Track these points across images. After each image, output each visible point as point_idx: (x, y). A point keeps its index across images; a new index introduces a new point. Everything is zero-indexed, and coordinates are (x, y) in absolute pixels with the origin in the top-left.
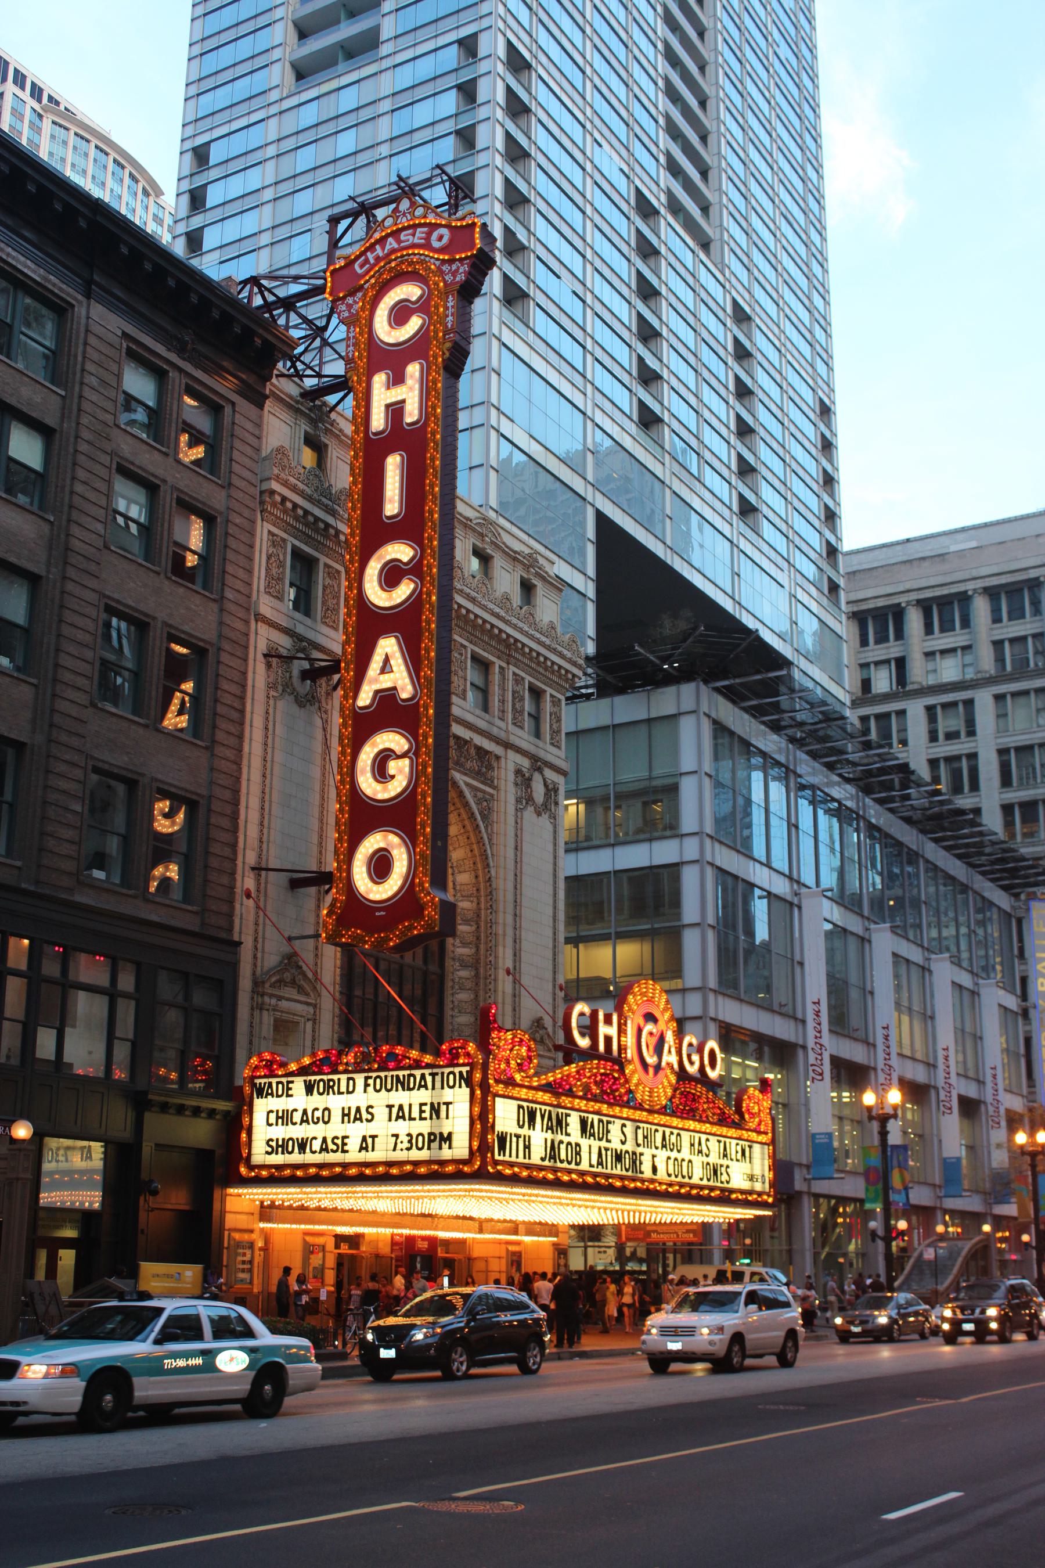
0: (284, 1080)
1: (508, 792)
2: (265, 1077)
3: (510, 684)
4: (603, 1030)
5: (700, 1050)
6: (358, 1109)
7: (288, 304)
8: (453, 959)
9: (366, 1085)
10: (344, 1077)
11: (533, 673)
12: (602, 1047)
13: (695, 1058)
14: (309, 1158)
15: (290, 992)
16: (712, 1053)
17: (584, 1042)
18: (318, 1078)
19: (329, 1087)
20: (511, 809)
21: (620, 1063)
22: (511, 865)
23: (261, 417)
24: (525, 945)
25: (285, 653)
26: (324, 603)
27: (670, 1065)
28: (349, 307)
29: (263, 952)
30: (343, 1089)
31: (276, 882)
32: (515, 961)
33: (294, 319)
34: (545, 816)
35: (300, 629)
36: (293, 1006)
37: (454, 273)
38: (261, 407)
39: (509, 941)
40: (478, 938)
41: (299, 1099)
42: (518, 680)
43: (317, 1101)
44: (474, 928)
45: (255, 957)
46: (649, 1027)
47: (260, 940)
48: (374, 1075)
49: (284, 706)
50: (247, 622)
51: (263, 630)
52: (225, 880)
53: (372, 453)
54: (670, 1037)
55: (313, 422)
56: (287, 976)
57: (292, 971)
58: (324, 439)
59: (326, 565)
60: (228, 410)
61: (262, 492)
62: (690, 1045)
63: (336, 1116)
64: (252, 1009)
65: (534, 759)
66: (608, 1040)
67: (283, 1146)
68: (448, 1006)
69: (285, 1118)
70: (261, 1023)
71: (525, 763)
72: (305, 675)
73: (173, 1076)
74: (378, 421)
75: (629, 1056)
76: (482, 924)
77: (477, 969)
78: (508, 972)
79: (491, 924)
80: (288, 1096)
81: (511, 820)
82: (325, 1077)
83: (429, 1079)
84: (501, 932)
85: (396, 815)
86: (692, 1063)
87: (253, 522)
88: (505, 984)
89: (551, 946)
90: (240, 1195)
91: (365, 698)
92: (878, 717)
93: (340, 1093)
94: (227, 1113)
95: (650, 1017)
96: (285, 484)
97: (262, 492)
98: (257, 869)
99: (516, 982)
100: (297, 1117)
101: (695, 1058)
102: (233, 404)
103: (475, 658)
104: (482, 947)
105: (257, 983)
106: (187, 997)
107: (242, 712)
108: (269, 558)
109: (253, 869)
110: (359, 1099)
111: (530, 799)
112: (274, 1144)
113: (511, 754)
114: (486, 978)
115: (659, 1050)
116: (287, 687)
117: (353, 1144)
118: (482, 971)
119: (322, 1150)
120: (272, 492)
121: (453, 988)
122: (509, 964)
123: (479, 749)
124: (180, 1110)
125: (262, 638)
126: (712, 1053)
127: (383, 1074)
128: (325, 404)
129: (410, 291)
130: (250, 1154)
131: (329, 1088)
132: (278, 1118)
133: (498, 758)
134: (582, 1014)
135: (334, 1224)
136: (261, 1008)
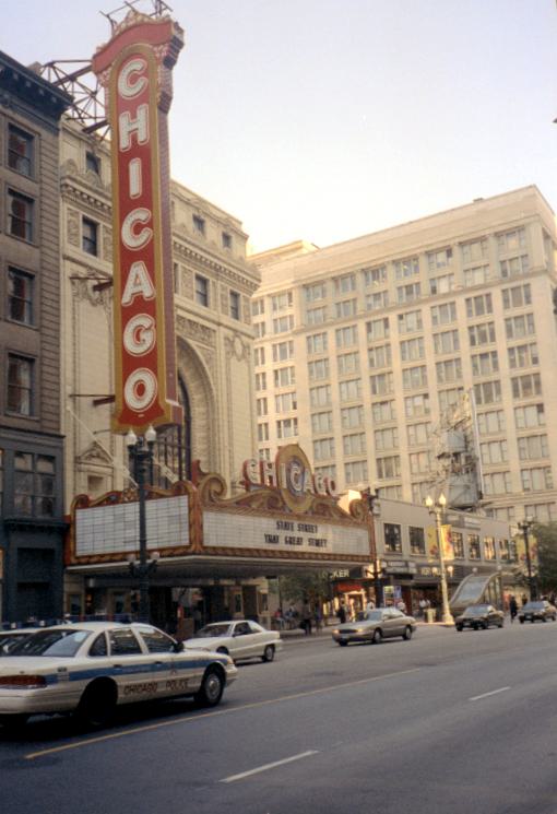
1: (222, 350)
3: (219, 291)
7: (72, 78)
11: (233, 284)
15: (95, 461)
20: (223, 358)
22: (225, 388)
23: (57, 143)
25: (82, 276)
26: (105, 248)
28: (105, 77)
31: (86, 402)
33: (77, 88)
34: (243, 361)
35: (90, 263)
36: (97, 467)
37: (161, 52)
38: (57, 135)
42: (223, 289)
49: (84, 305)
50: (58, 260)
51: (68, 263)
52: (54, 402)
53: (123, 160)
55: (92, 146)
58: (97, 155)
59: (104, 227)
60: (37, 137)
61: (61, 186)
65: (235, 331)
71: (230, 333)
72: (96, 288)
74: (125, 143)
81: (223, 364)
85: (149, 361)
87: (57, 203)
91: (127, 299)
92: (440, 306)
96: (74, 180)
97: (61, 186)
98: (74, 396)
102: (40, 135)
103: (199, 278)
105: (77, 460)
107: (58, 309)
108: (69, 222)
109: (71, 396)
111: (234, 352)
113: (222, 328)
116: (86, 295)
120: (67, 185)
123: (203, 327)
125: (68, 269)
128: (97, 135)
129: (136, 65)
130: (75, 551)
133: (214, 331)
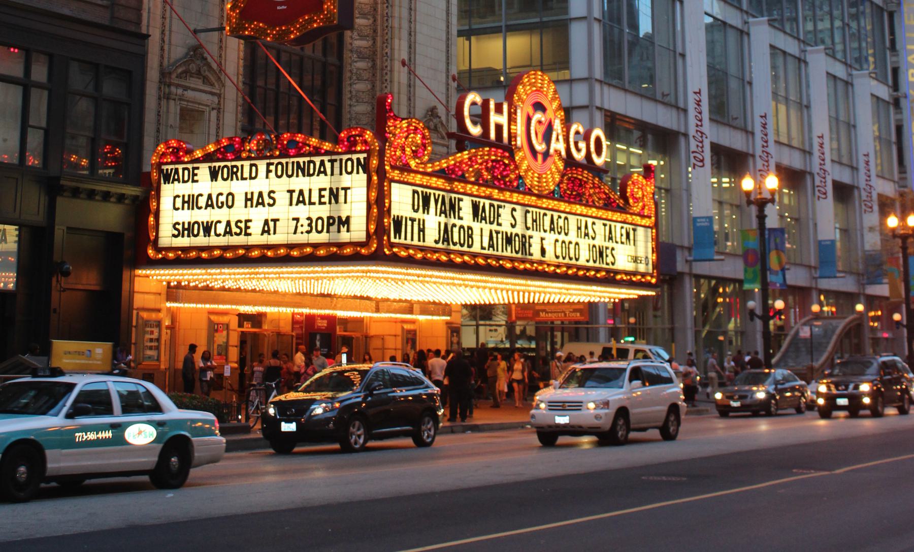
0: (190, 166)
2: (172, 163)
4: (494, 118)
5: (587, 138)
6: (261, 195)
8: (351, 51)
9: (268, 171)
10: (247, 164)
12: (493, 135)
13: (582, 145)
14: (213, 240)
16: (598, 141)
17: (475, 130)
18: (222, 164)
19: (233, 173)
21: (510, 150)
24: (420, 38)
27: (557, 152)
29: (170, 44)
30: (246, 175)
32: (410, 53)
39: (405, 34)
40: (375, 31)
41: (204, 185)
43: (221, 186)
44: (371, 21)
45: (162, 49)
46: (538, 116)
47: (167, 33)
48: (276, 161)
54: (558, 125)
56: (193, 67)
57: (197, 64)
62: (577, 133)
63: (240, 200)
64: (160, 99)
66: (499, 128)
67: (189, 229)
68: (346, 96)
69: (191, 202)
70: (168, 112)
73: (84, 162)
75: (519, 143)
76: (379, 18)
77: (374, 61)
78: (404, 64)
79: (387, 17)
80: (193, 181)
82: (229, 164)
83: (328, 165)
84: (396, 25)
86: (578, 150)
88: (401, 75)
89: (444, 38)
90: (147, 276)
93: (243, 179)
94: (136, 197)
95: (539, 107)
99: (411, 72)
100: (202, 202)
101: (582, 145)
104: (379, 39)
105: (164, 74)
106: (98, 87)
110: (261, 184)
112: (180, 227)
114: (382, 69)
115: (547, 137)
117: (256, 228)
118: (378, 62)
119: (226, 233)
121: (350, 78)
122: (405, 56)
124: (91, 195)
126: (598, 141)
127: (284, 161)
131: (233, 174)
132: (184, 202)
134: (474, 104)
135: (237, 304)
136: (168, 97)
